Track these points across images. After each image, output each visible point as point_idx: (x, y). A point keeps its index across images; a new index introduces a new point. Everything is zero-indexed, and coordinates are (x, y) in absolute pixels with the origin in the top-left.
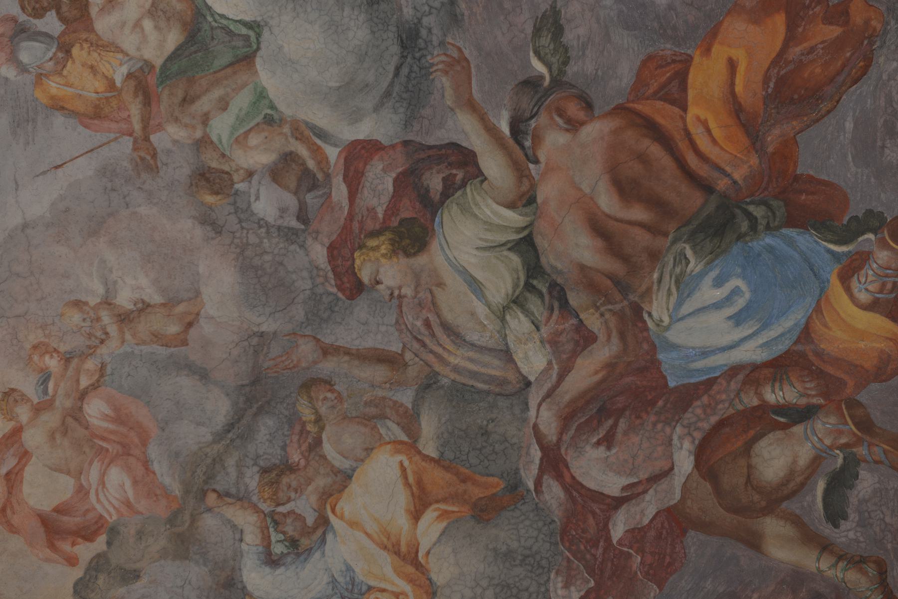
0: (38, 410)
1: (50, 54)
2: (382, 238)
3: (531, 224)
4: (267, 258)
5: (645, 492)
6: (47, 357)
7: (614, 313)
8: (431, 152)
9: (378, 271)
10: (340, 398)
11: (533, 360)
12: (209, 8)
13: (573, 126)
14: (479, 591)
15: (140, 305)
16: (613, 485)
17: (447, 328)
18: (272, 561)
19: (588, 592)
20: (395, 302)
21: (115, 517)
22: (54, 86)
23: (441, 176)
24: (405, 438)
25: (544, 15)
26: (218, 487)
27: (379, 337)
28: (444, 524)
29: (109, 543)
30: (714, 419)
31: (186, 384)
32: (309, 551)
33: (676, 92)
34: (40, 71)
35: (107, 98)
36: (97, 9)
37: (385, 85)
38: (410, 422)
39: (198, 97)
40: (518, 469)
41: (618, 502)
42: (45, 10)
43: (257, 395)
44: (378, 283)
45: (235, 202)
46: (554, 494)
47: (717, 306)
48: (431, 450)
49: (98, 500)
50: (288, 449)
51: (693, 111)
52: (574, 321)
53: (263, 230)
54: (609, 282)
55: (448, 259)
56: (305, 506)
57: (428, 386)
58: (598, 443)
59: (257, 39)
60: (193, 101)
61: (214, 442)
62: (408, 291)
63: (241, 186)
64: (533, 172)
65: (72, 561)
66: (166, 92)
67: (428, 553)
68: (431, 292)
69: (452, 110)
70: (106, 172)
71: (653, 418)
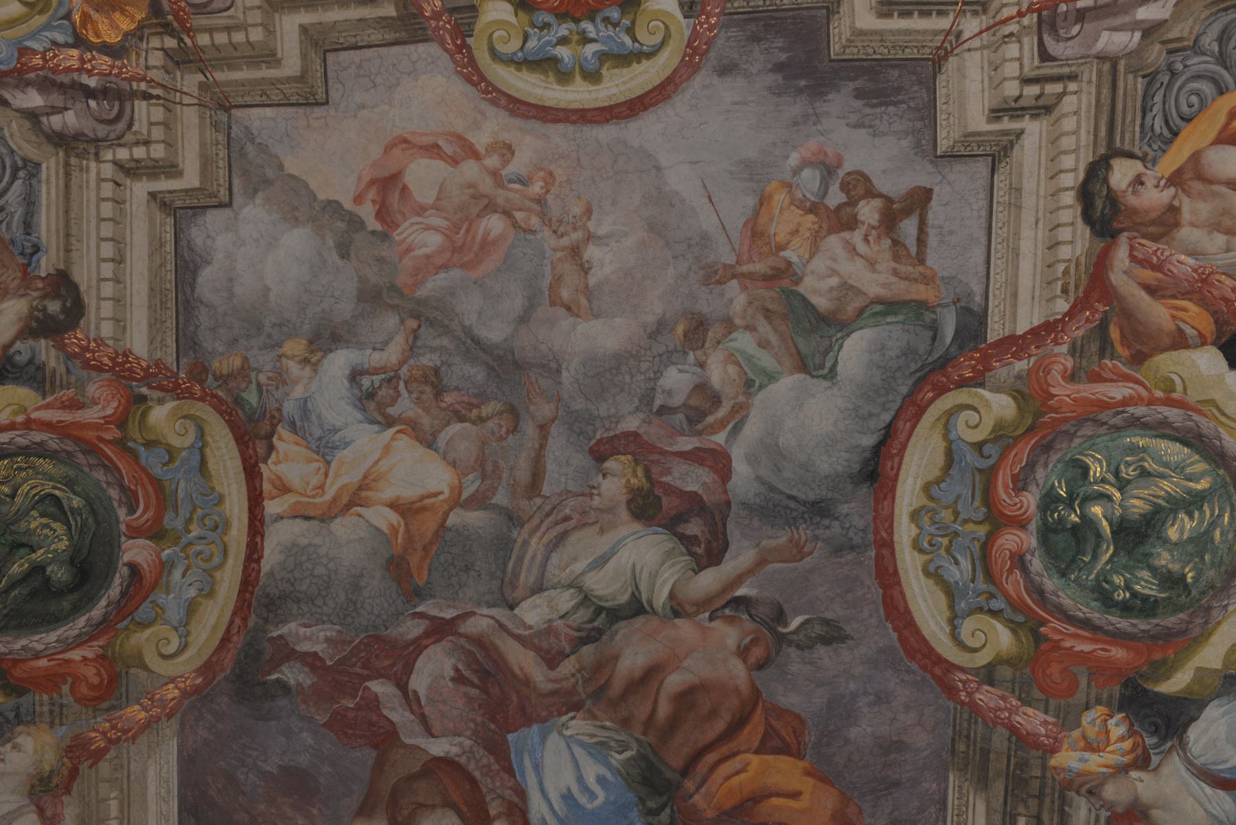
0: (495, 174)
1: (809, 196)
2: (644, 480)
3: (655, 613)
4: (627, 378)
5: (412, 712)
6: (542, 184)
7: (574, 686)
8: (720, 525)
9: (614, 475)
11: (533, 613)
12: (848, 335)
14: (325, 561)
15: (586, 266)
16: (419, 683)
17: (563, 536)
18: (355, 376)
19: (321, 659)
20: (587, 490)
21: (397, 238)
22: (780, 198)
23: (699, 535)
25: (841, 628)
26: (422, 329)
27: (556, 475)
28: (386, 531)
29: (373, 232)
30: (477, 774)
31: (516, 304)
32: (363, 410)
33: (771, 744)
37: (781, 487)
38: (479, 501)
39: (770, 323)
40: (433, 596)
41: (403, 687)
42: (848, 193)
43: (505, 365)
44: (604, 475)
45: (677, 351)
46: (412, 629)
47: (580, 779)
48: (452, 520)
49: (413, 224)
50: (455, 393)
51: (755, 760)
52: (568, 650)
53: (652, 375)
54: (603, 682)
55: (625, 538)
56: (404, 406)
57: (511, 518)
58: (457, 670)
60: (766, 318)
61: (463, 327)
62: (596, 502)
63: (691, 357)
64: (701, 616)
65: (358, 199)
66: (775, 295)
67: (360, 516)
68: (596, 522)
69: (758, 545)
70: (705, 240)
71: (479, 719)
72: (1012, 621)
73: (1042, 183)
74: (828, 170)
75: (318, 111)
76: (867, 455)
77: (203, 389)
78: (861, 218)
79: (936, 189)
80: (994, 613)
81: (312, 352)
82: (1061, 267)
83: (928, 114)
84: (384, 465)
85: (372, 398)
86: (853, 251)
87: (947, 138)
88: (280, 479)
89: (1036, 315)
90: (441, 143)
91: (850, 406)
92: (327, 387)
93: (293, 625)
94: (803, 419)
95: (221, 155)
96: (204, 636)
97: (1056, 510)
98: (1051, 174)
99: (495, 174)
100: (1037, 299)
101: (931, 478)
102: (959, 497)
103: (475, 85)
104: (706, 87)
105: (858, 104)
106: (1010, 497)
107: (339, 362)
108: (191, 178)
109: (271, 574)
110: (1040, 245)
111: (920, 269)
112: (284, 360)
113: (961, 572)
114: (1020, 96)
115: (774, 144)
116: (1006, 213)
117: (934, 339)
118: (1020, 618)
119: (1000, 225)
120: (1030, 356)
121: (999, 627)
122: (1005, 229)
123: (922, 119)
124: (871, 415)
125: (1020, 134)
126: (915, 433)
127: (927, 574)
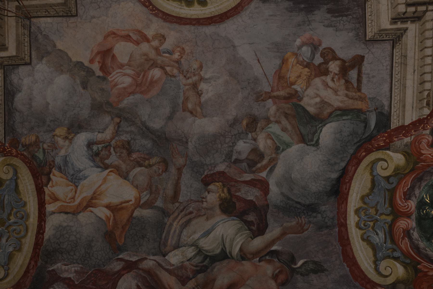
0: (157, 49)
1: (305, 59)
2: (227, 194)
3: (233, 258)
4: (220, 146)
6: (179, 54)
9: (213, 192)
10: (159, 175)
11: (174, 258)
12: (324, 125)
13: (275, 277)
14: (75, 233)
15: (200, 92)
18: (90, 145)
19: (73, 281)
20: (200, 199)
21: (110, 79)
22: (292, 60)
23: (254, 220)
24: (141, 202)
26: (122, 123)
28: (104, 219)
29: (99, 77)
31: (167, 111)
32: (93, 161)
34: (298, 55)
35: (287, 82)
36: (324, 79)
37: (293, 198)
38: (149, 205)
39: (287, 119)
40: (127, 251)
44: (209, 192)
45: (243, 133)
46: (117, 266)
48: (136, 213)
49: (117, 73)
50: (138, 153)
52: (191, 276)
53: (231, 144)
55: (218, 222)
56: (113, 159)
59: (311, 145)
62: (205, 205)
63: (250, 135)
64: (255, 260)
65: (92, 61)
67: (92, 212)
69: (282, 226)
70: (256, 80)
72: (403, 262)
73: (417, 53)
74: (315, 47)
75: (72, 20)
76: (334, 182)
77: (17, 151)
78: (330, 70)
79: (366, 56)
80: (396, 259)
81: (69, 134)
82: (426, 93)
83: (362, 21)
84: (103, 188)
85: (98, 155)
86: (326, 85)
87: (371, 32)
88: (53, 193)
89: (414, 115)
90: (131, 34)
91: (326, 159)
92: (76, 150)
93: (59, 265)
94: (303, 165)
95: (26, 40)
96: (16, 270)
97: (425, 209)
98: (420, 49)
99: (157, 49)
100: (414, 108)
101: (365, 193)
102: (378, 202)
103: (147, 7)
104: (256, 8)
105: (329, 16)
106: (403, 203)
107: (83, 138)
108: (12, 51)
109: (49, 240)
110: (416, 82)
111: (359, 94)
112: (56, 137)
113: (379, 239)
114: (406, 12)
115: (289, 35)
116: (399, 67)
117: (365, 127)
118: (408, 261)
119: (397, 73)
120: (411, 135)
121: (398, 265)
122: (399, 75)
123: (359, 23)
124: (336, 163)
125: (406, 30)
126: (357, 172)
127: (363, 239)
